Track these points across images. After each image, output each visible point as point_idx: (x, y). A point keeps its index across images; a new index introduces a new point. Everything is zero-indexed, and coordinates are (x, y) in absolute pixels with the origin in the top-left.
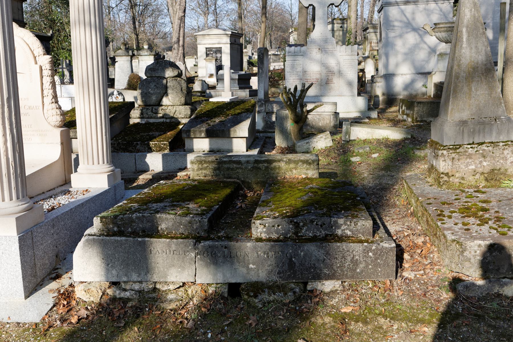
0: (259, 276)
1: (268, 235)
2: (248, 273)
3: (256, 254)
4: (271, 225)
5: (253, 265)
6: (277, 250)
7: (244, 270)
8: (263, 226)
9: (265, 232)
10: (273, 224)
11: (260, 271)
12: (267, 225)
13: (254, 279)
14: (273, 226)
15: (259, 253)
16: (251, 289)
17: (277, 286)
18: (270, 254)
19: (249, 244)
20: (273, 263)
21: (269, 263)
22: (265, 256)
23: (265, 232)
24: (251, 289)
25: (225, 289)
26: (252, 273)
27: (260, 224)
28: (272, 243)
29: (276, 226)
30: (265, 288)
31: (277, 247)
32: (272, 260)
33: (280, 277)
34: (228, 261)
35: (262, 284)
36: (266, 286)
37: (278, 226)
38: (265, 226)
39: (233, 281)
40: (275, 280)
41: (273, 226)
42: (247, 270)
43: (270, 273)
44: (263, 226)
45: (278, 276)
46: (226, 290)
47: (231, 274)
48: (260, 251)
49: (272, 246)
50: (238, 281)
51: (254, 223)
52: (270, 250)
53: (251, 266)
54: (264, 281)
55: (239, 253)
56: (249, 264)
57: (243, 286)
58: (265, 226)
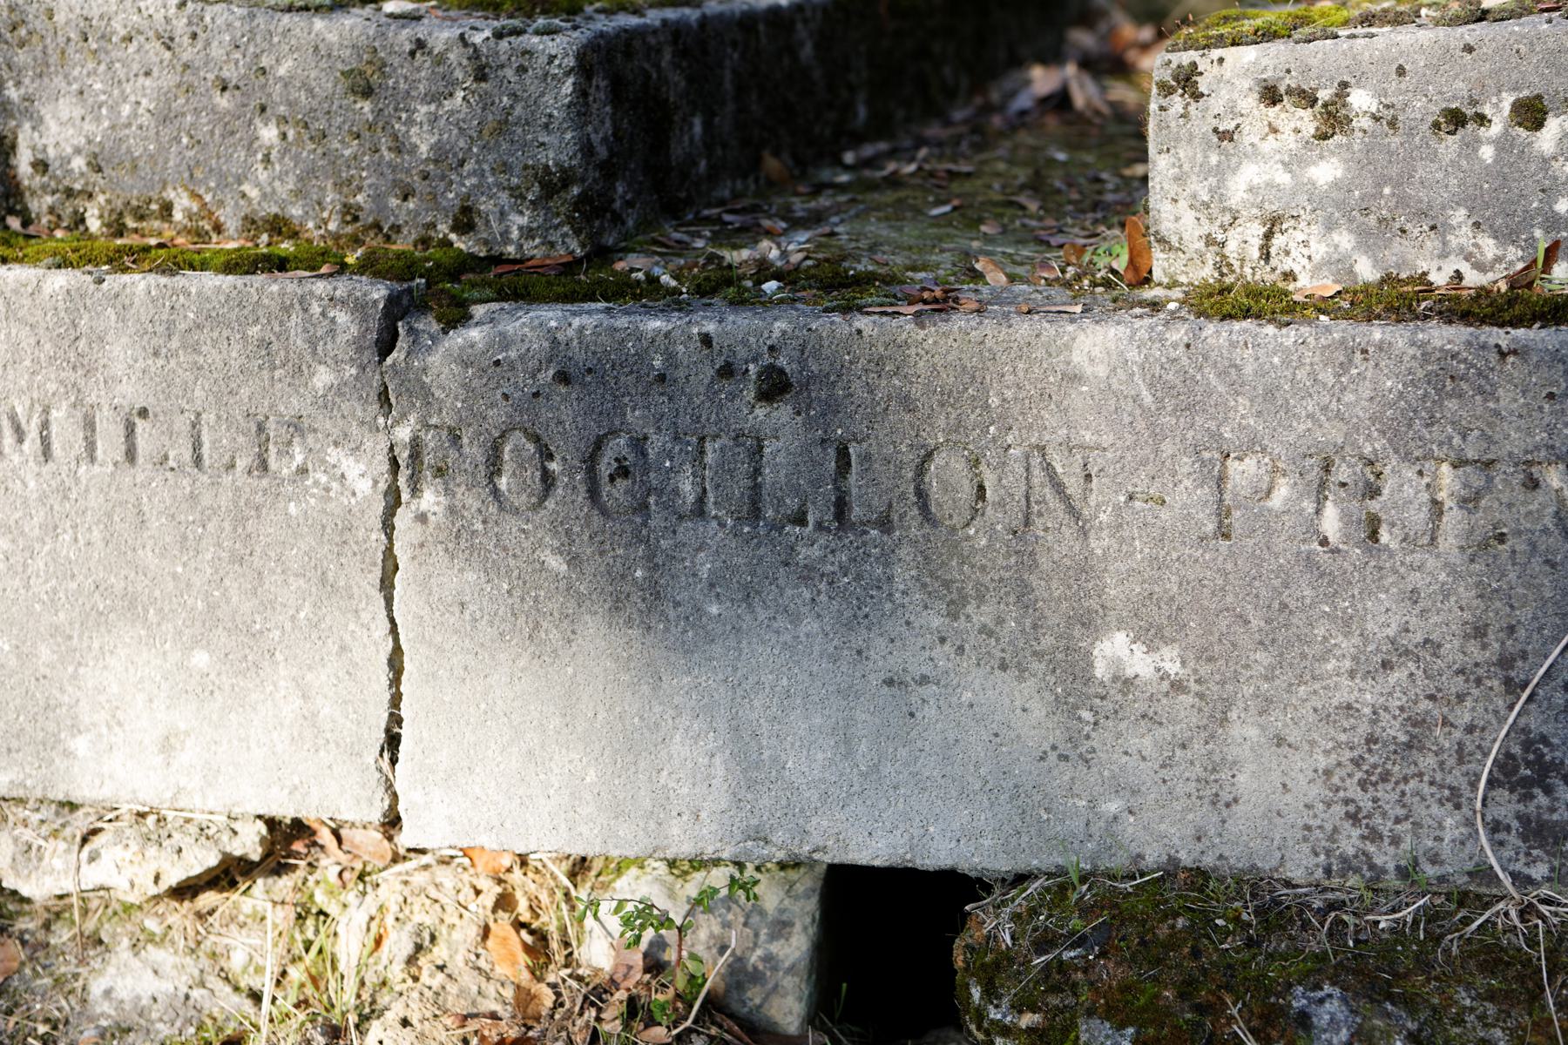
0: (1224, 803)
1: (1366, 239)
2: (1073, 751)
3: (1188, 496)
4: (1423, 108)
5: (1151, 637)
6: (1514, 440)
7: (1023, 708)
8: (1306, 120)
9: (1336, 208)
10: (1456, 92)
11: (1245, 731)
12: (1361, 100)
13: (1159, 833)
14: (1456, 119)
15: (1244, 471)
16: (1110, 972)
17: (1491, 955)
18: (1403, 489)
19: (1098, 345)
20: (1446, 622)
21: (1384, 617)
22: (1331, 522)
23: (1336, 208)
24: (1110, 972)
25: (781, 927)
26: (1133, 748)
27: (1271, 95)
28: (1442, 335)
29: (1499, 109)
30: (1317, 971)
31: (1507, 399)
32: (1430, 572)
33: (1538, 832)
34: (808, 574)
35: (1273, 908)
36: (1318, 942)
37: (1531, 114)
38: (1334, 119)
39: (873, 849)
40: (1455, 866)
41: (1456, 119)
42: (1065, 706)
43: (1384, 759)
44: (1306, 120)
45: (1506, 806)
46: (796, 947)
47: (847, 743)
48: (1253, 445)
49: (1443, 376)
50: (938, 854)
51: (1187, 80)
52: (1408, 428)
53: (1116, 651)
54: (1300, 866)
55: (949, 470)
56: (1089, 623)
57: (993, 924)
58: (1334, 119)
